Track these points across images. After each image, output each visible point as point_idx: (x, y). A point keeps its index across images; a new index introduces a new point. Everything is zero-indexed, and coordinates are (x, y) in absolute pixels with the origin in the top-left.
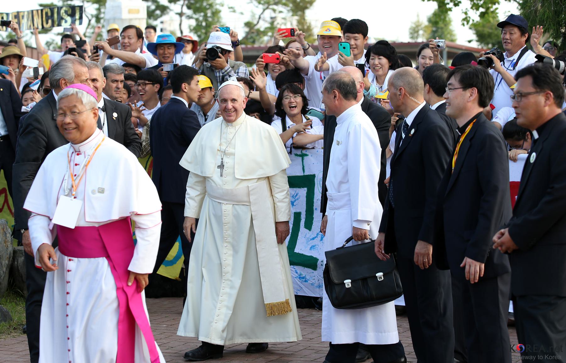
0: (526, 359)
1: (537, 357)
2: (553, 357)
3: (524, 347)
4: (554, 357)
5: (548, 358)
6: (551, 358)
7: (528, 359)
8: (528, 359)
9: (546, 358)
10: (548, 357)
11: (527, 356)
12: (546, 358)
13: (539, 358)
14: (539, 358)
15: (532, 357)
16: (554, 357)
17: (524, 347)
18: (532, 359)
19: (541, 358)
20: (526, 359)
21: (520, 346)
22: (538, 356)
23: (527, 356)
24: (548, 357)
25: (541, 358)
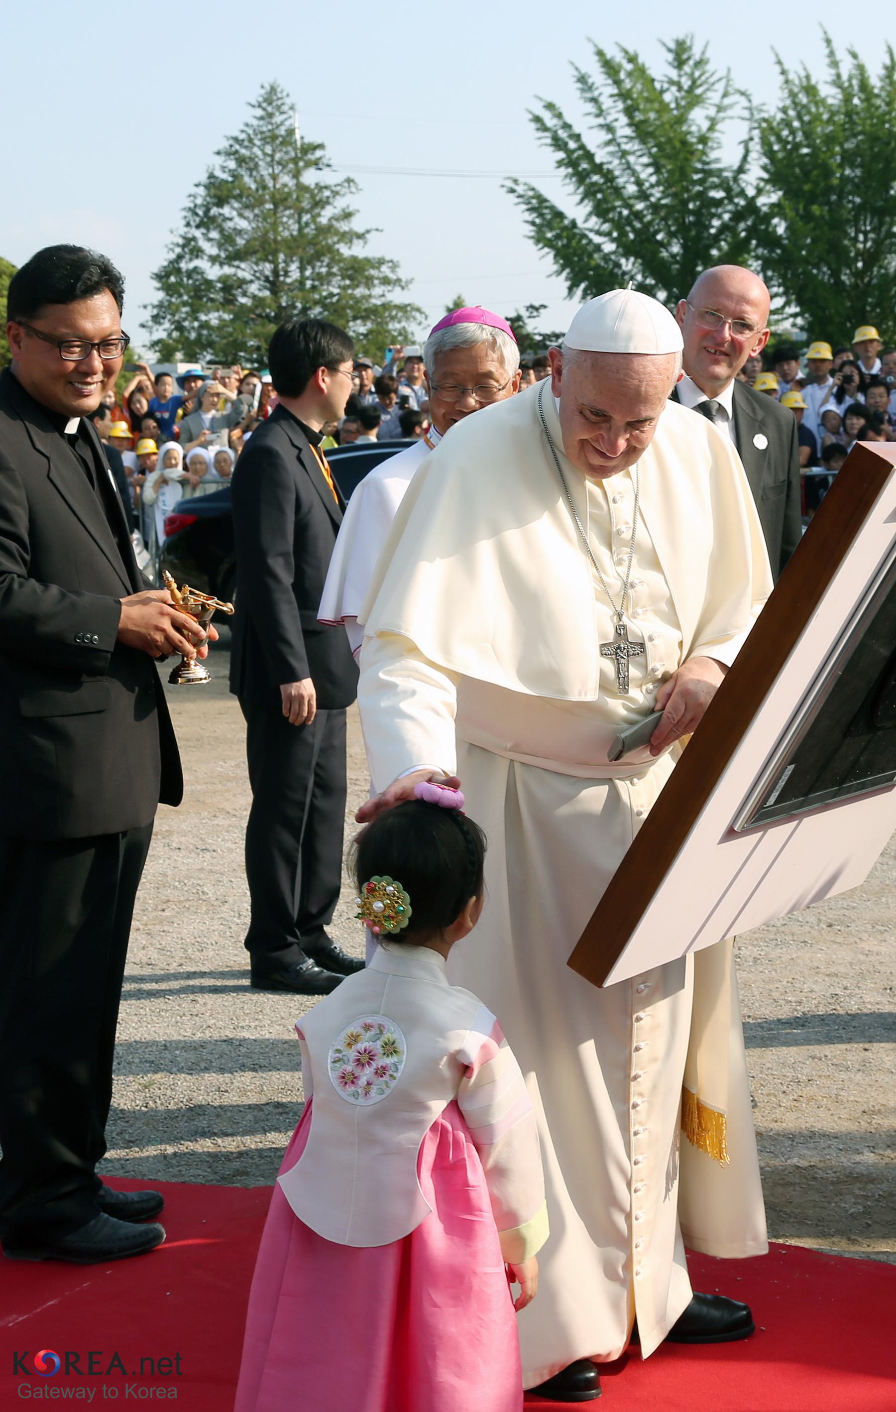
0: (65, 1397)
1: (100, 1392)
2: (151, 1389)
3: (57, 1360)
4: (154, 1392)
5: (137, 1395)
6: (143, 1393)
7: (71, 1396)
8: (71, 1396)
9: (130, 1393)
10: (136, 1390)
11: (68, 1389)
12: (130, 1393)
13: (107, 1395)
14: (107, 1395)
15: (84, 1392)
16: (154, 1392)
17: (57, 1360)
18: (84, 1396)
19: (113, 1393)
20: (65, 1397)
21: (45, 1355)
22: (105, 1388)
23: (68, 1389)
24: (136, 1390)
25: (113, 1393)
